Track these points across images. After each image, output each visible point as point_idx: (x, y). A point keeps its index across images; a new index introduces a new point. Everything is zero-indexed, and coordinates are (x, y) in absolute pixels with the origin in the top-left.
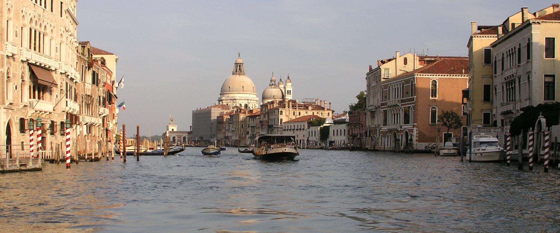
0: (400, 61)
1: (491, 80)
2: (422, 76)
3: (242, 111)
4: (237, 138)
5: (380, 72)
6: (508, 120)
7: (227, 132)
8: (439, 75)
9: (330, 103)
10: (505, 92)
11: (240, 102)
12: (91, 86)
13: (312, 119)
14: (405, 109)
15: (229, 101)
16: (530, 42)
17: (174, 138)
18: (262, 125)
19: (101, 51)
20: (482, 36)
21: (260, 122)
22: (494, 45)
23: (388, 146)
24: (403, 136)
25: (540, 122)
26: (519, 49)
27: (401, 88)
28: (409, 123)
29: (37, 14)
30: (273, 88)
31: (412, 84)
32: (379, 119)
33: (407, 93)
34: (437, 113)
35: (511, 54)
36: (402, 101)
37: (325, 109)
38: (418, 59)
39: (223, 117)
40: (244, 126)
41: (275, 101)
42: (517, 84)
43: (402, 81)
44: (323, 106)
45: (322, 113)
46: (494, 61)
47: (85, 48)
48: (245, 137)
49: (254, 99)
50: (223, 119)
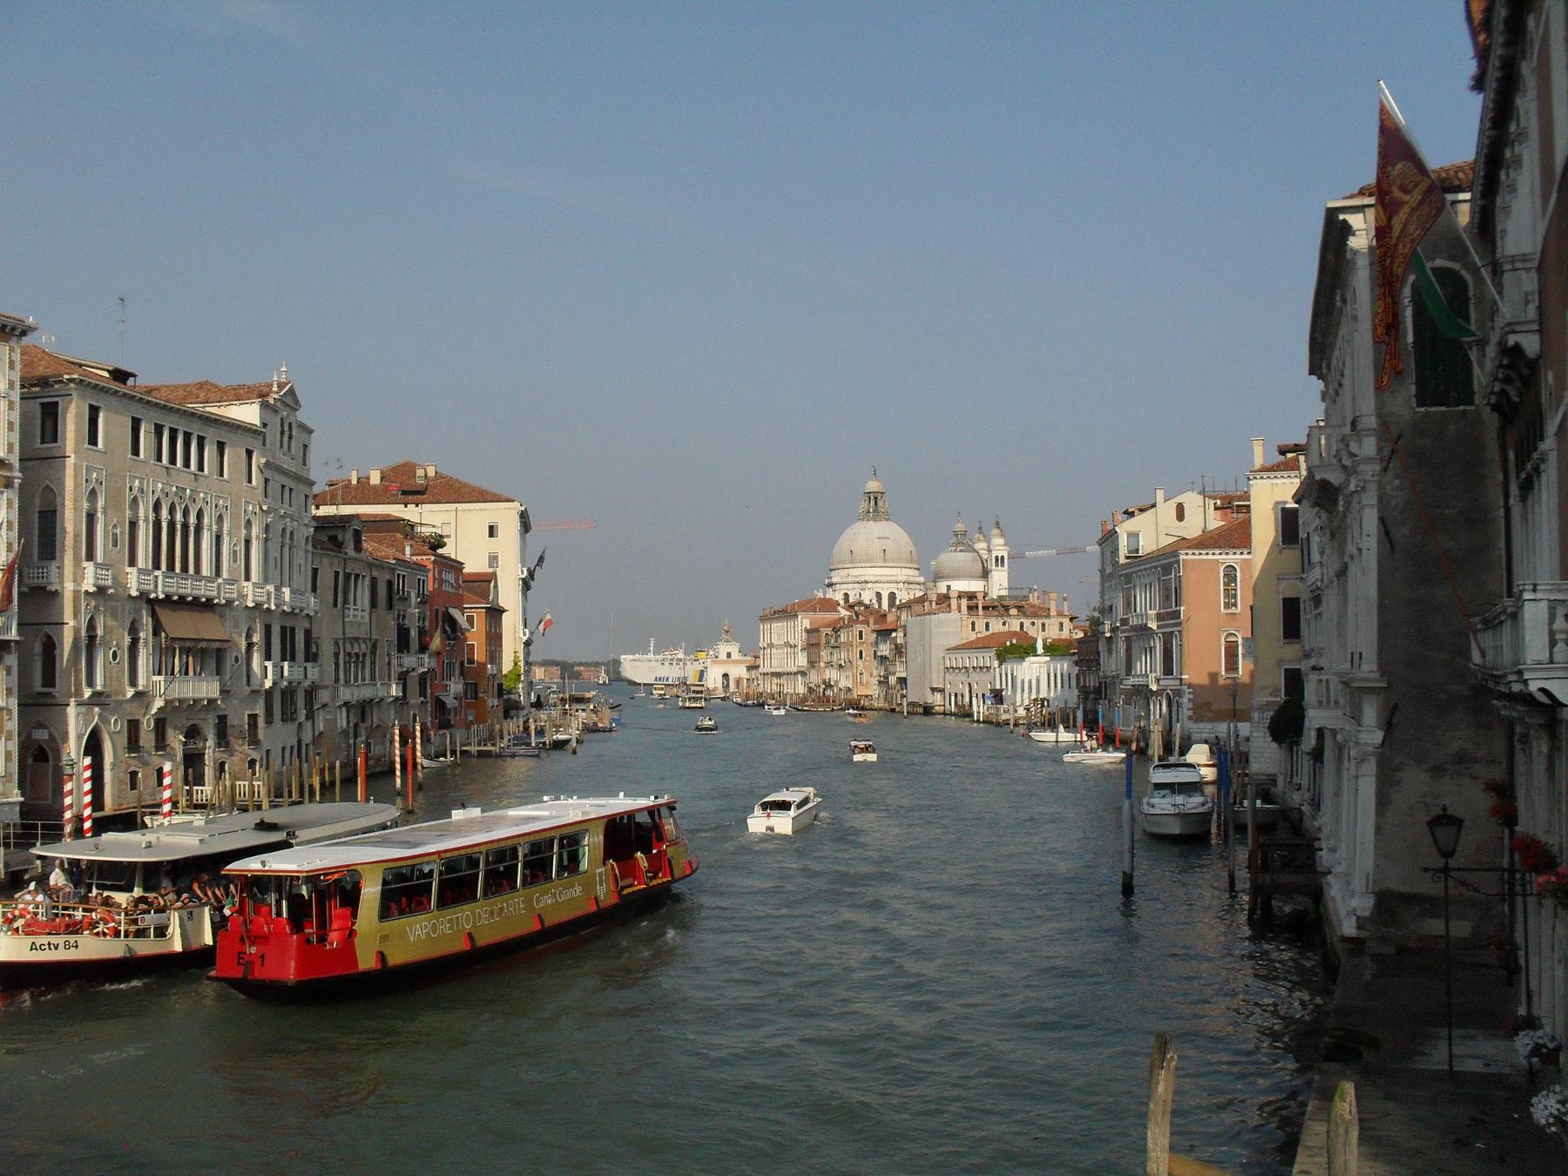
0: (1166, 510)
1: (1298, 583)
2: (1198, 557)
3: (861, 618)
8: (1242, 553)
11: (878, 587)
12: (366, 614)
15: (850, 586)
17: (726, 676)
30: (961, 551)
34: (1240, 648)
37: (1053, 612)
40: (867, 655)
43: (1156, 567)
45: (1043, 625)
49: (912, 579)
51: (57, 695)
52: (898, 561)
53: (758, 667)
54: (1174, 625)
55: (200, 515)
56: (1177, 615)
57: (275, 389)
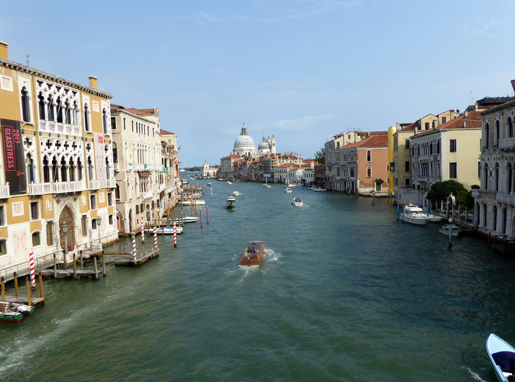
0: (346, 137)
1: (409, 158)
4: (247, 175)
5: (334, 144)
6: (423, 187)
7: (240, 172)
9: (300, 155)
10: (421, 168)
11: (245, 151)
13: (291, 166)
14: (351, 168)
15: (239, 151)
16: (440, 142)
17: (208, 172)
18: (261, 169)
19: (167, 132)
20: (403, 132)
21: (260, 166)
22: (412, 138)
23: (341, 188)
24: (350, 183)
25: (451, 198)
26: (431, 145)
27: (348, 154)
28: (354, 176)
29: (141, 141)
31: (355, 154)
32: (334, 172)
33: (352, 158)
35: (425, 146)
36: (349, 163)
37: (298, 159)
38: (357, 135)
39: (237, 163)
40: (250, 168)
41: (268, 155)
42: (430, 166)
43: (349, 151)
44: (296, 156)
45: (296, 161)
46: (412, 147)
47: (165, 148)
48: (251, 175)
49: (254, 149)
50: (237, 164)
51: (120, 200)
52: (250, 145)
53: (220, 171)
54: (355, 165)
55: (146, 146)
56: (356, 163)
57: (155, 111)
